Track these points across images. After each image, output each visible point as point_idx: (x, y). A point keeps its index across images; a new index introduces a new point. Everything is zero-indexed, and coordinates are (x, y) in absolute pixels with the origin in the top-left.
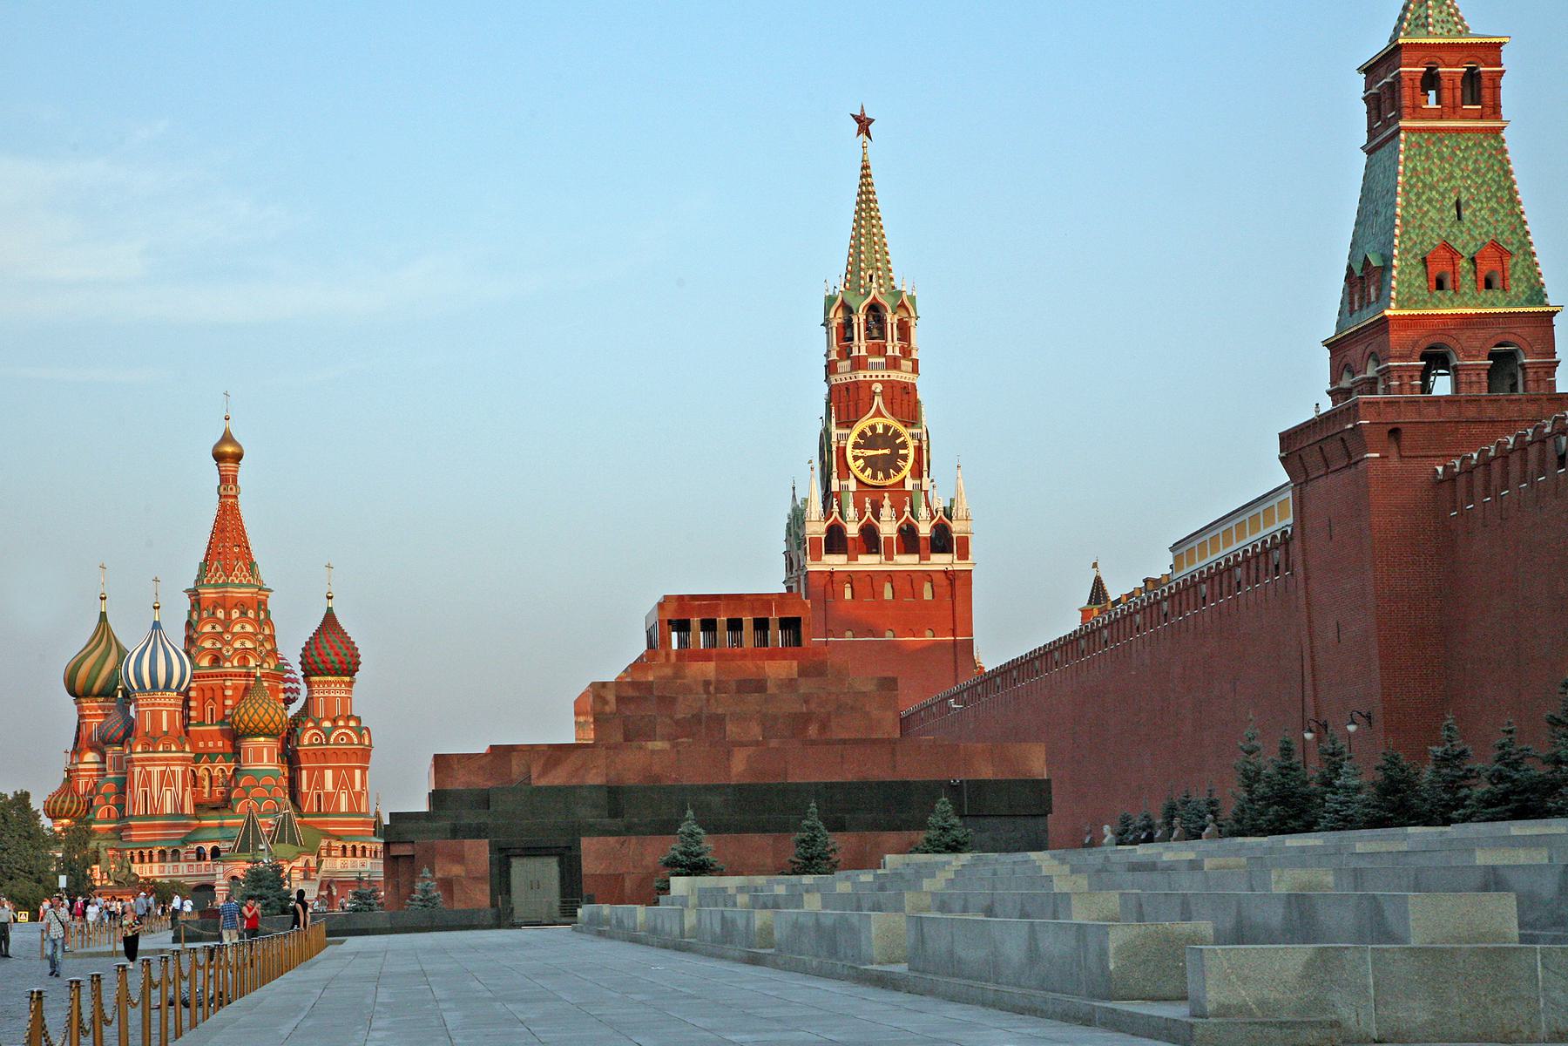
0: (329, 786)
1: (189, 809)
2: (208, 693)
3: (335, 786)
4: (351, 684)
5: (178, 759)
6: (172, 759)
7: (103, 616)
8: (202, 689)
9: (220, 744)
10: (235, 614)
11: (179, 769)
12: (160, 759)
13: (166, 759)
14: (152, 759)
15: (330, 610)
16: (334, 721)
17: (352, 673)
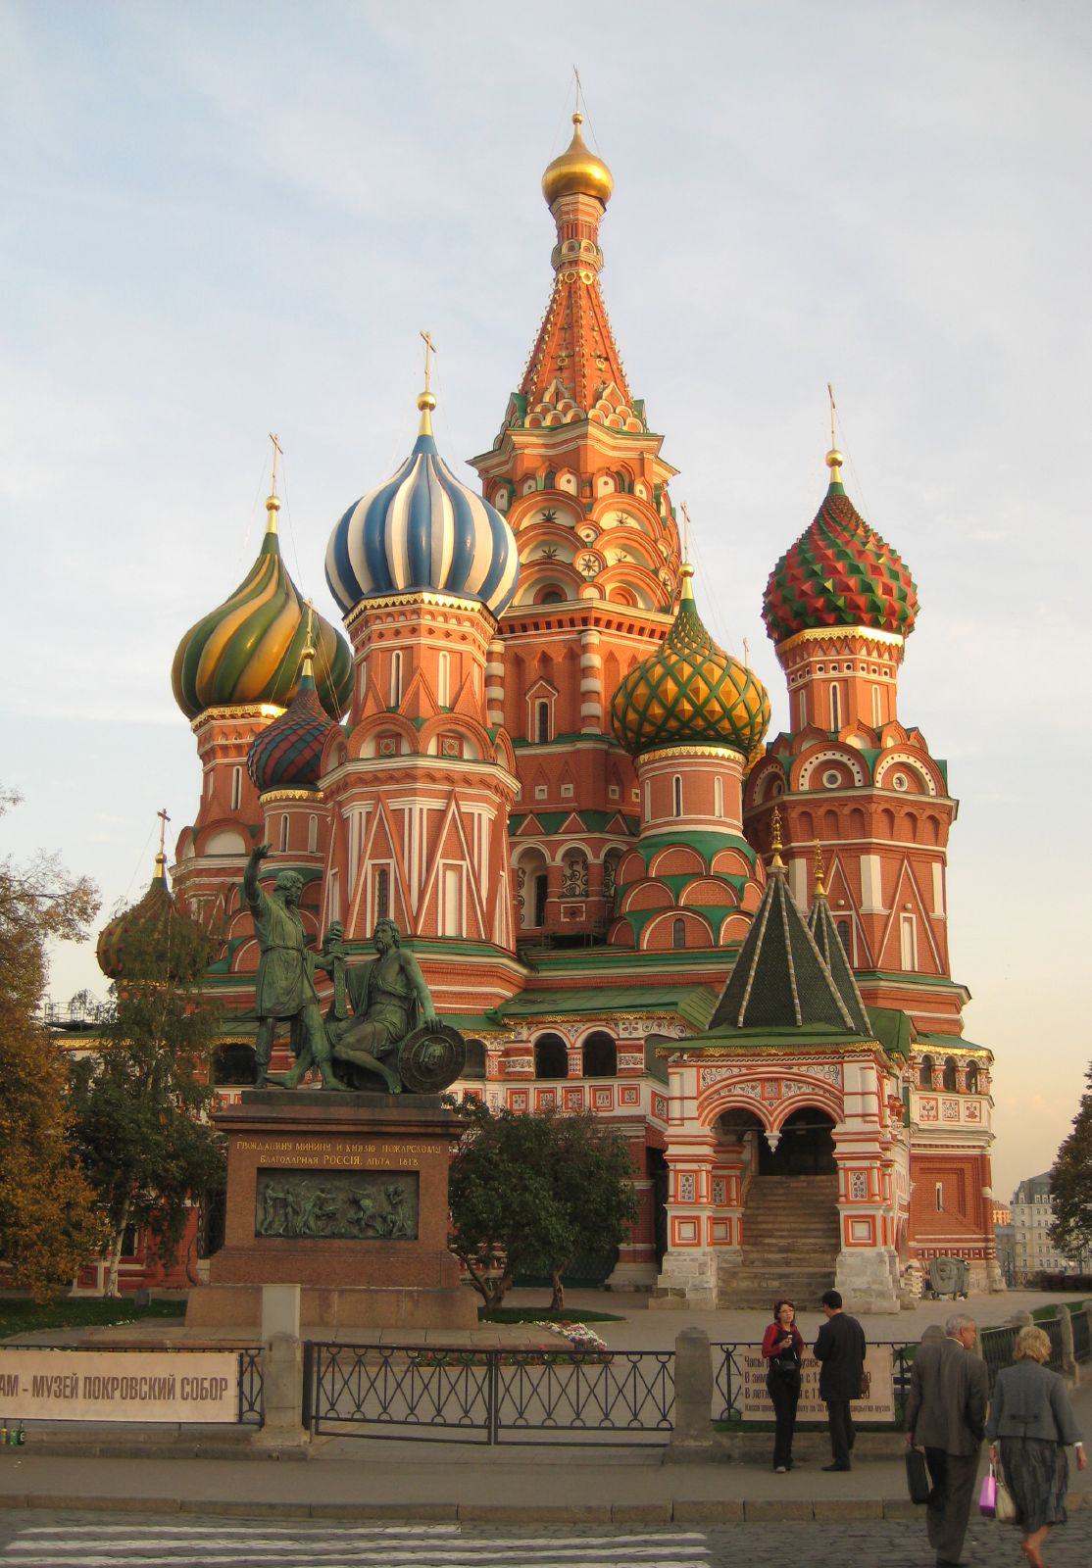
0: (874, 899)
1: (503, 936)
2: (533, 666)
3: (889, 903)
4: (897, 654)
5: (484, 782)
6: (467, 781)
7: (270, 542)
8: (516, 661)
9: (568, 790)
10: (604, 487)
11: (484, 812)
12: (431, 777)
13: (449, 779)
14: (409, 775)
15: (834, 487)
16: (876, 736)
17: (901, 622)
